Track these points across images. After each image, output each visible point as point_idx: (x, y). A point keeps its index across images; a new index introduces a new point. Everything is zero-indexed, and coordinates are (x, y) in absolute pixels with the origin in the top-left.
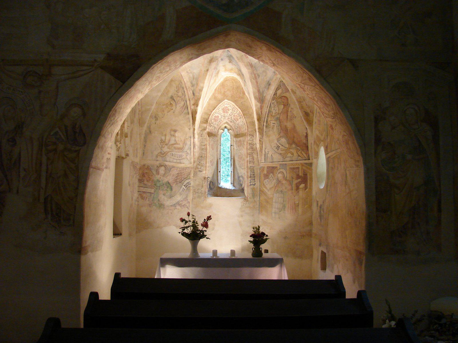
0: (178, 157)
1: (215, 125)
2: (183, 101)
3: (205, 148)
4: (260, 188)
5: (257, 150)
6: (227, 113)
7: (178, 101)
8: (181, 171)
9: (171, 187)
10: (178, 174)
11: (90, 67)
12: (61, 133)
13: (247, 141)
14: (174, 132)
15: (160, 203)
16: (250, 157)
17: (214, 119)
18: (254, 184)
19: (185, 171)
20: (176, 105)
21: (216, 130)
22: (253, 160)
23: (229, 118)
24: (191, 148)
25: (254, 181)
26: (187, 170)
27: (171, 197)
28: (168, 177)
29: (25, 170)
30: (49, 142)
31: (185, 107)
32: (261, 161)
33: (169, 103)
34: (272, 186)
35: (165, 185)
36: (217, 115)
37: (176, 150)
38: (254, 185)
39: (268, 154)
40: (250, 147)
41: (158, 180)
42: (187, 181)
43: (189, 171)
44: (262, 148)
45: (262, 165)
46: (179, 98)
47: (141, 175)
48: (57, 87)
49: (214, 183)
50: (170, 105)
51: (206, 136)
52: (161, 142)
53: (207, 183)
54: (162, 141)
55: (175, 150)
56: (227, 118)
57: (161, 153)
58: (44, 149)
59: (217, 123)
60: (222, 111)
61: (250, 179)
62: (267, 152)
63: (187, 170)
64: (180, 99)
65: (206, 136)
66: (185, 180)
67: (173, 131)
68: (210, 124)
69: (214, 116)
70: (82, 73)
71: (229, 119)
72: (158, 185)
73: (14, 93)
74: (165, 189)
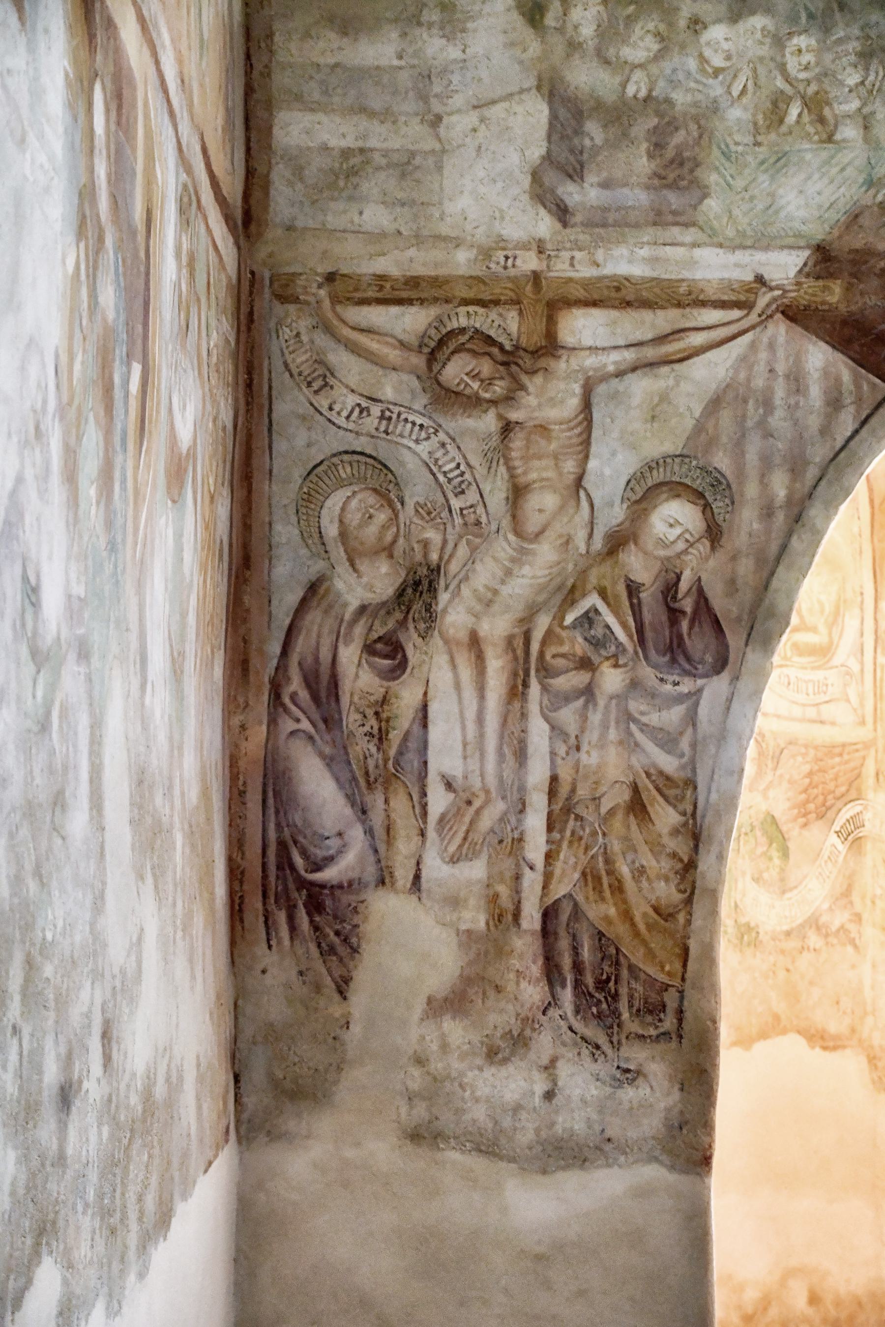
0: (811, 691)
8: (821, 760)
10: (810, 774)
11: (736, 313)
12: (611, 619)
15: (743, 920)
19: (837, 760)
24: (862, 645)
26: (846, 757)
27: (784, 892)
29: (449, 786)
30: (554, 656)
42: (848, 812)
48: (587, 405)
55: (796, 659)
58: (535, 688)
63: (846, 757)
66: (839, 804)
70: (697, 339)
73: (387, 432)
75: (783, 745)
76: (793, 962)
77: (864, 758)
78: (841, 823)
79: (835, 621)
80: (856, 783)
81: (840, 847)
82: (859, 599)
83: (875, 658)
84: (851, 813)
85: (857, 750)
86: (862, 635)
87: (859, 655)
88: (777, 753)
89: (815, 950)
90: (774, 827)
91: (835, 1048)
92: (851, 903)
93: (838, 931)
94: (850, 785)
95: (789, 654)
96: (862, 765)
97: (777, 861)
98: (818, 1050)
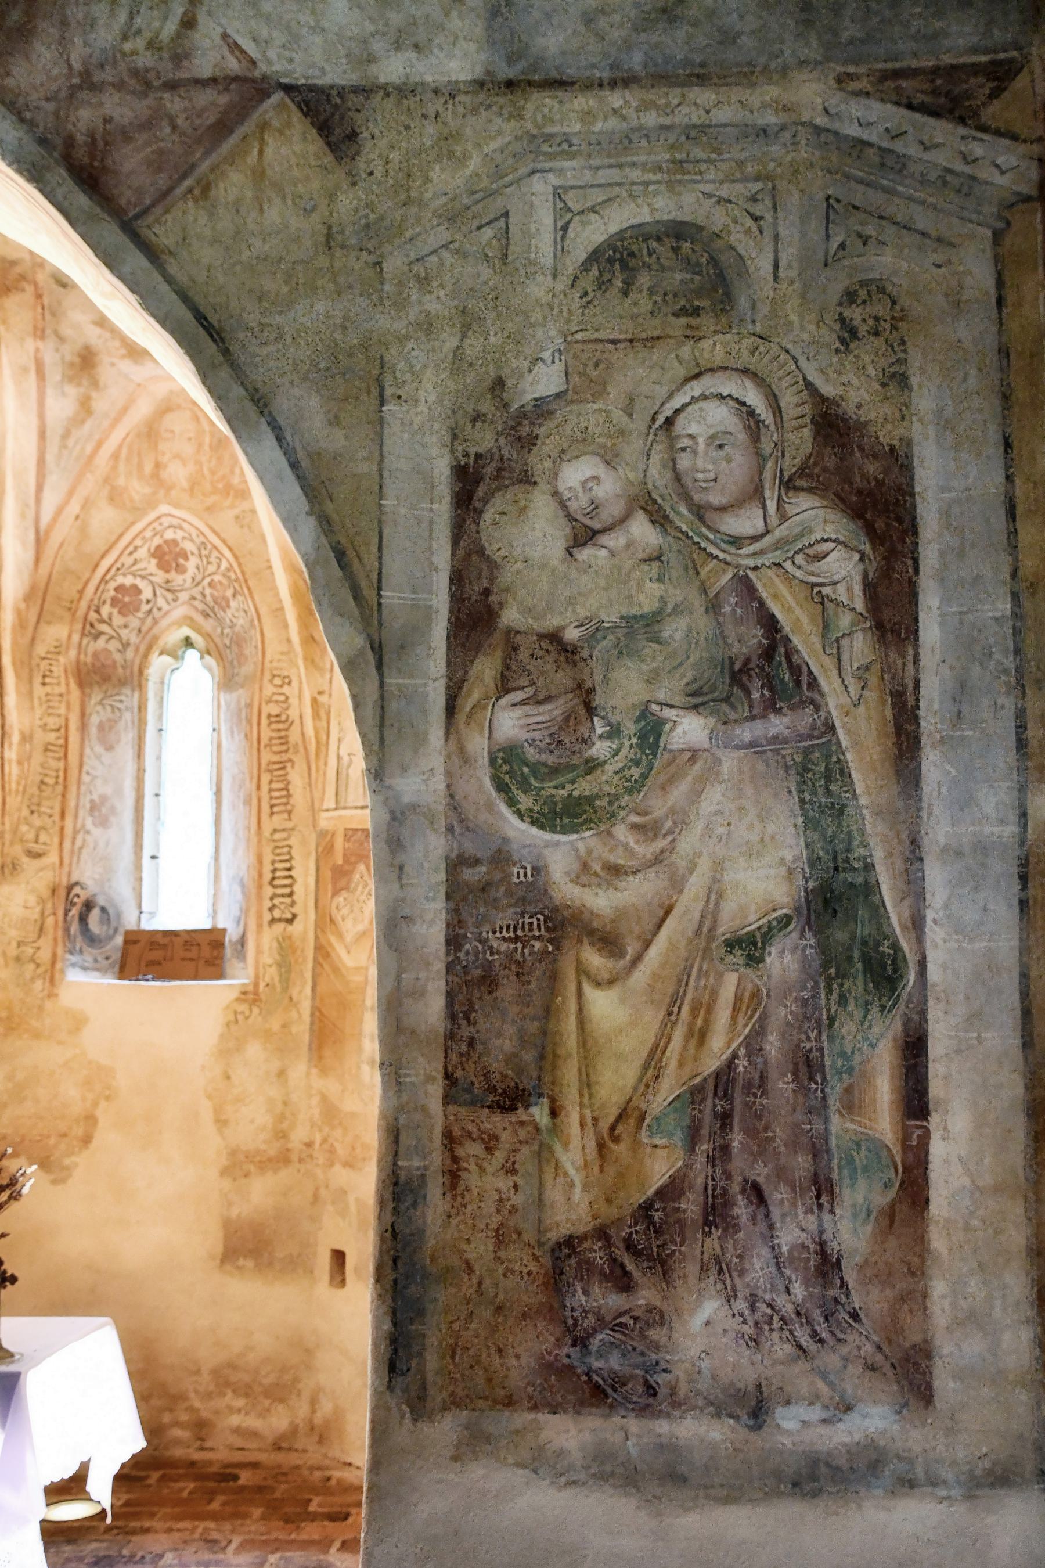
1: (124, 633)
3: (61, 742)
4: (317, 938)
5: (305, 748)
6: (180, 569)
13: (260, 705)
16: (271, 782)
17: (114, 602)
18: (289, 916)
21: (130, 654)
22: (284, 800)
23: (194, 598)
25: (288, 900)
32: (322, 800)
34: (360, 927)
36: (128, 581)
38: (290, 921)
39: (349, 766)
40: (275, 735)
44: (324, 738)
45: (325, 821)
49: (111, 911)
51: (67, 685)
53: (66, 912)
56: (183, 596)
59: (134, 623)
60: (154, 561)
61: (269, 891)
62: (346, 759)
68: (92, 625)
69: (112, 585)
71: (196, 603)
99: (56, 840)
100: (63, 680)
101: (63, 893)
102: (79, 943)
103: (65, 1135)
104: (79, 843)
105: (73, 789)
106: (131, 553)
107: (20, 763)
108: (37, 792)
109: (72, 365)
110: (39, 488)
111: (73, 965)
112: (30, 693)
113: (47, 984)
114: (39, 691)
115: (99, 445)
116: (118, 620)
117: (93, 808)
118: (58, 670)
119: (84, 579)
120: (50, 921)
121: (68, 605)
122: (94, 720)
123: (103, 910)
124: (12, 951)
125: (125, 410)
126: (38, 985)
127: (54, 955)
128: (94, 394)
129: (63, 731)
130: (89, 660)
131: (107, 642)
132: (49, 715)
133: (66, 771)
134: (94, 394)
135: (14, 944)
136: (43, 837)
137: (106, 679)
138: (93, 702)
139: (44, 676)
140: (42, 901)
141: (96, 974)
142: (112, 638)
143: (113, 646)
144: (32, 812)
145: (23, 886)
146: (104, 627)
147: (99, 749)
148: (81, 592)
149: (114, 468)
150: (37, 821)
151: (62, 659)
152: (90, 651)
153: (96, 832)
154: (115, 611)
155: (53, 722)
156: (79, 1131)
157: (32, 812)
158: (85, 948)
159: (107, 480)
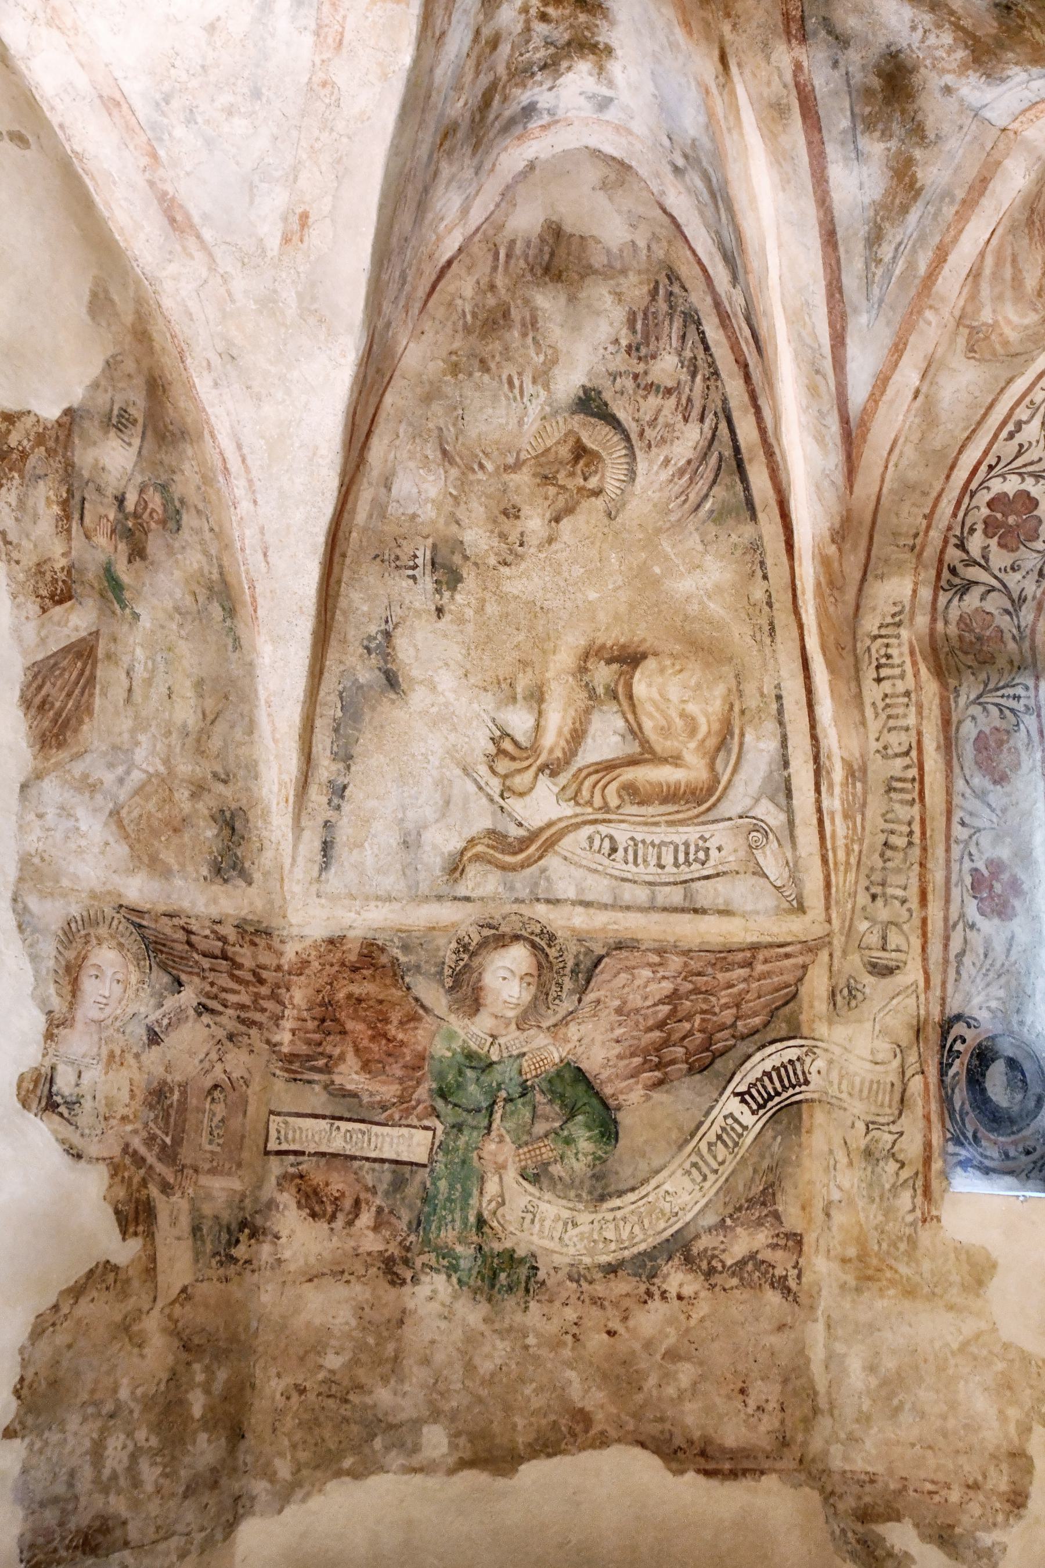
0: (668, 859)
1: (1013, 580)
2: (695, 414)
3: (913, 772)
7: (653, 423)
8: (699, 974)
9: (606, 1107)
10: (673, 998)
14: (615, 666)
19: (743, 972)
20: (632, 455)
24: (788, 781)
26: (760, 968)
27: (602, 1198)
28: (573, 1031)
31: (713, 460)
33: (565, 452)
35: (539, 1098)
36: (1011, 486)
37: (650, 810)
41: (470, 1056)
43: (789, 978)
46: (654, 401)
47: (311, 1025)
50: (577, 458)
51: (916, 674)
52: (501, 752)
53: (943, 1069)
54: (507, 745)
55: (634, 809)
57: (494, 835)
63: (760, 968)
64: (672, 401)
65: (916, 674)
66: (743, 1047)
67: (609, 662)
68: (953, 571)
69: (985, 497)
72: (474, 1093)
74: (540, 1128)
75: (600, 951)
76: (625, 1319)
77: (805, 967)
78: (751, 1079)
79: (722, 744)
80: (787, 1010)
81: (748, 1119)
82: (774, 706)
83: (818, 801)
84: (776, 1061)
85: (787, 956)
86: (786, 764)
87: (782, 799)
88: (588, 963)
89: (680, 1297)
90: (581, 1088)
91: (734, 1474)
92: (776, 1216)
93: (742, 1263)
94: (772, 1014)
95: (613, 801)
96: (801, 980)
97: (585, 1145)
98: (690, 1476)
99: (916, 942)
100: (908, 667)
101: (933, 1035)
102: (972, 1122)
103: (975, 1486)
104: (955, 946)
105: (938, 851)
106: (1011, 436)
107: (846, 816)
108: (879, 864)
109: (868, 93)
110: (838, 340)
111: (964, 1164)
112: (859, 695)
113: (919, 1199)
114: (872, 692)
115: (941, 256)
116: (999, 559)
117: (978, 884)
118: (900, 653)
119: (934, 494)
120: (916, 1085)
121: (911, 542)
122: (969, 730)
123: (1012, 1064)
124: (859, 1140)
125: (981, 185)
126: (906, 1196)
127: (928, 1146)
128: (918, 154)
129: (914, 754)
130: (953, 630)
131: (983, 598)
132: (890, 730)
133: (923, 821)
134: (918, 154)
135: (861, 1126)
136: (895, 939)
137: (987, 660)
138: (962, 700)
139: (878, 667)
140: (901, 1050)
141: (1009, 1180)
142: (993, 589)
143: (995, 603)
144: (874, 897)
145: (868, 1025)
146: (974, 573)
147: (978, 781)
148: (929, 517)
149: (974, 296)
150: (883, 913)
151: (905, 633)
152: (954, 614)
153: (987, 926)
154: (993, 542)
155: (897, 741)
156: (1000, 1481)
157: (874, 897)
158: (982, 1131)
159: (959, 322)
